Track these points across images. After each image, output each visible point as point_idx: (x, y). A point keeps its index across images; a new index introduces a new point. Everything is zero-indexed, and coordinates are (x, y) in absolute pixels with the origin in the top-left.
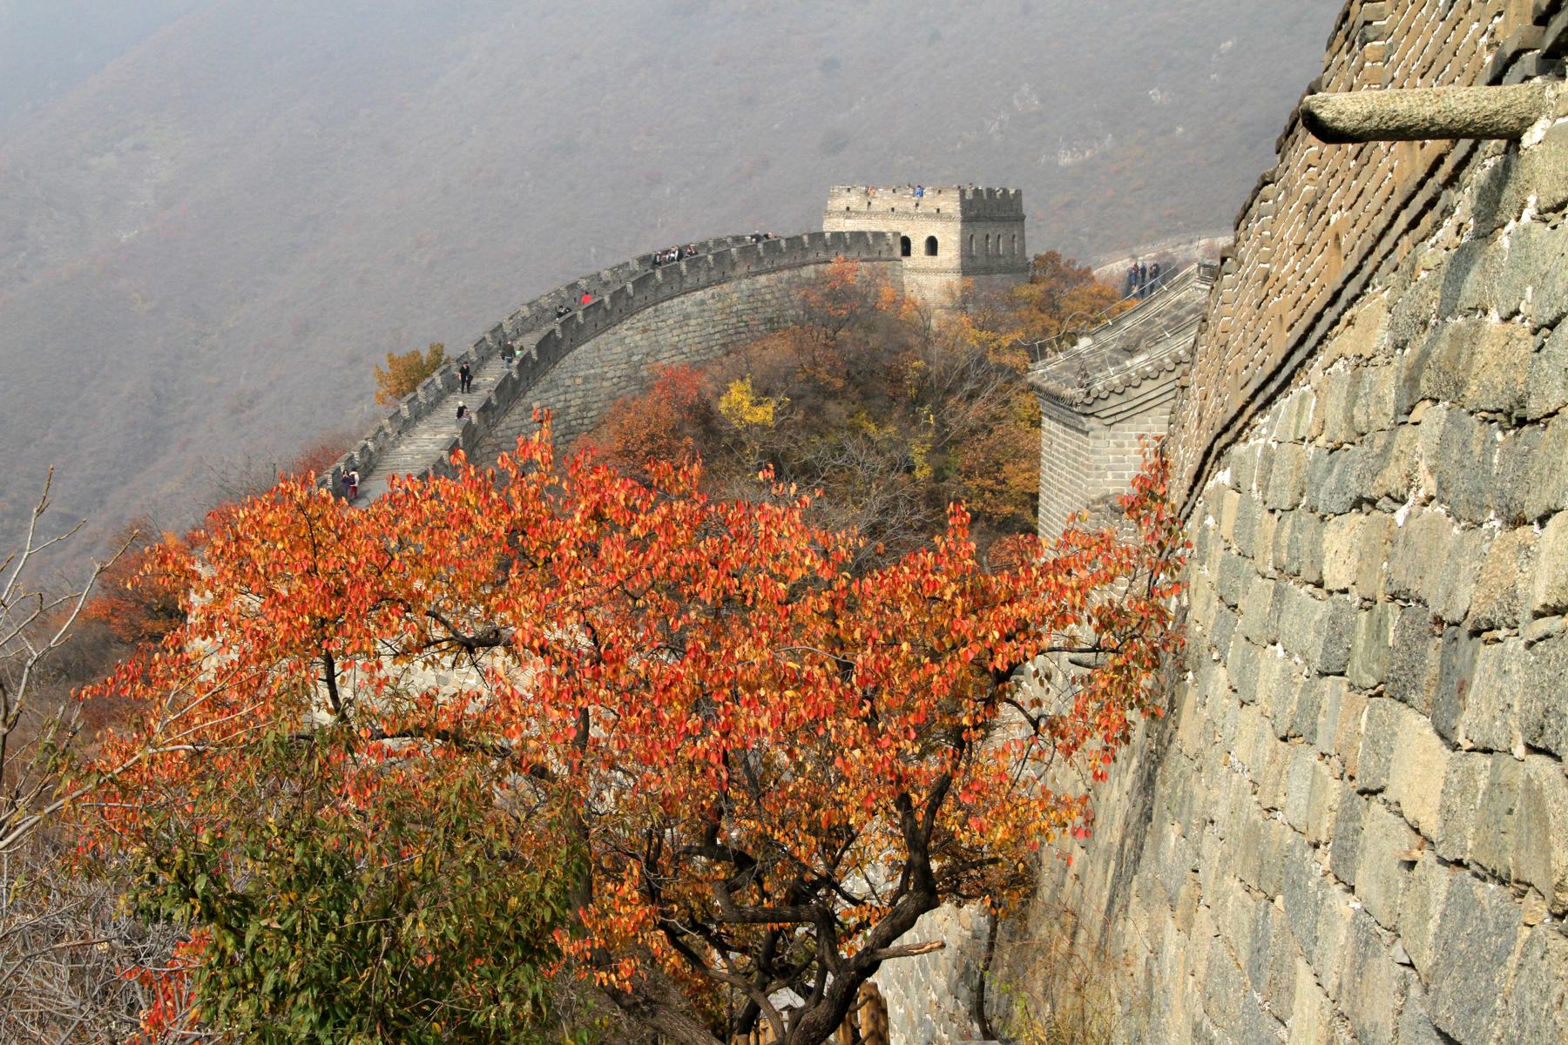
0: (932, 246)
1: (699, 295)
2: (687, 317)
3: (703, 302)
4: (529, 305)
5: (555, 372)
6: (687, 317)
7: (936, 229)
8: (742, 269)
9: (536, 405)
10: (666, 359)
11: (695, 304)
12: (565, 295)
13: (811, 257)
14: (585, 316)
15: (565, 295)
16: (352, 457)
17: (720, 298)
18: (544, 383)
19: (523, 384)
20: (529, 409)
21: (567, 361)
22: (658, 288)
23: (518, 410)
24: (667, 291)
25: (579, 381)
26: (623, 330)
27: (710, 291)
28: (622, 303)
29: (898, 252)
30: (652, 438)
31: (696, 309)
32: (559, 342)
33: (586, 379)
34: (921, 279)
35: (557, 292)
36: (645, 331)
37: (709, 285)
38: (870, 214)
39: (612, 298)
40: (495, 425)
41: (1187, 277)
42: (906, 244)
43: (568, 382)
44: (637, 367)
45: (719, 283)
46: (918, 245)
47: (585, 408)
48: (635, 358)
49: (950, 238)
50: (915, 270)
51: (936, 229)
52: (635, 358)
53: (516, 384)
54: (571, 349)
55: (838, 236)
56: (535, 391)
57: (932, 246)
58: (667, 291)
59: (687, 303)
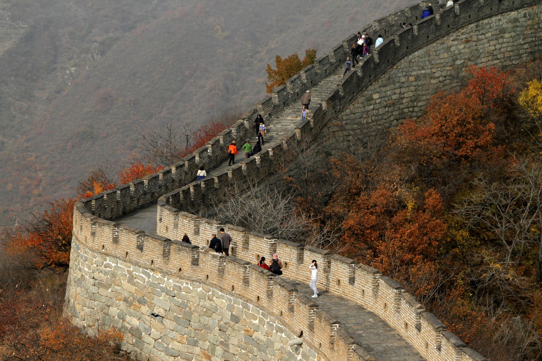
1: (514, 14)
2: (503, 31)
3: (516, 20)
4: (380, 21)
5: (393, 72)
6: (503, 31)
9: (376, 96)
10: (484, 62)
11: (510, 21)
12: (408, 14)
14: (419, 30)
15: (408, 14)
16: (230, 133)
17: (531, 17)
18: (383, 79)
19: (366, 80)
20: (370, 99)
21: (403, 63)
22: (480, 8)
23: (361, 99)
24: (487, 11)
25: (412, 79)
26: (449, 41)
27: (522, 12)
28: (450, 20)
30: (462, 123)
31: (510, 25)
32: (397, 49)
33: (417, 78)
35: (402, 12)
36: (467, 41)
37: (522, 7)
39: (442, 16)
40: (341, 111)
43: (403, 79)
44: (458, 69)
47: (415, 99)
48: (458, 62)
52: (458, 62)
53: (360, 80)
54: (407, 54)
56: (376, 85)
58: (487, 11)
59: (502, 21)
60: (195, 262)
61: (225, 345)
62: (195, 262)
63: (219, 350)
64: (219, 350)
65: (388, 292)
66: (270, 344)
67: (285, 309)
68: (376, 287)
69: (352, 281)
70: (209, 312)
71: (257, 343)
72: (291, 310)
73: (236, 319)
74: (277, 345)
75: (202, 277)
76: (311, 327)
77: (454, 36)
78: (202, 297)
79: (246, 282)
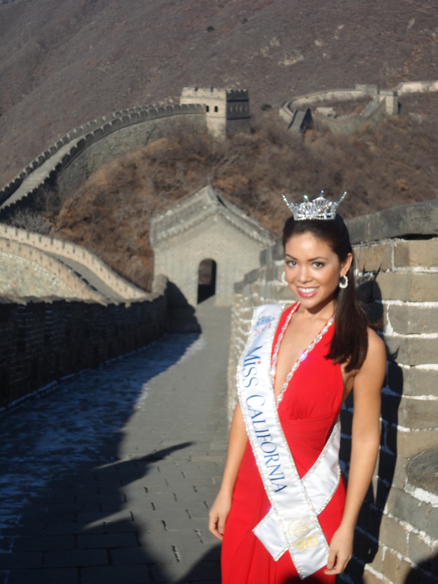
0: (216, 109)
6: (130, 133)
7: (218, 104)
8: (149, 117)
13: (174, 112)
17: (143, 127)
20: (74, 166)
27: (139, 124)
29: (205, 110)
34: (213, 120)
38: (196, 97)
41: (204, 191)
42: (207, 109)
45: (141, 122)
46: (212, 109)
49: (222, 107)
50: (211, 117)
51: (218, 104)
55: (184, 106)
56: (76, 159)
57: (216, 109)
60: (8, 245)
61: (23, 279)
62: (8, 245)
63: (20, 281)
64: (20, 281)
65: (89, 257)
66: (42, 278)
67: (48, 264)
68: (84, 255)
69: (74, 251)
70: (15, 266)
71: (36, 278)
72: (51, 264)
73: (27, 268)
74: (45, 278)
75: (11, 251)
76: (59, 271)
77: (110, 136)
78: (12, 259)
79: (31, 253)
